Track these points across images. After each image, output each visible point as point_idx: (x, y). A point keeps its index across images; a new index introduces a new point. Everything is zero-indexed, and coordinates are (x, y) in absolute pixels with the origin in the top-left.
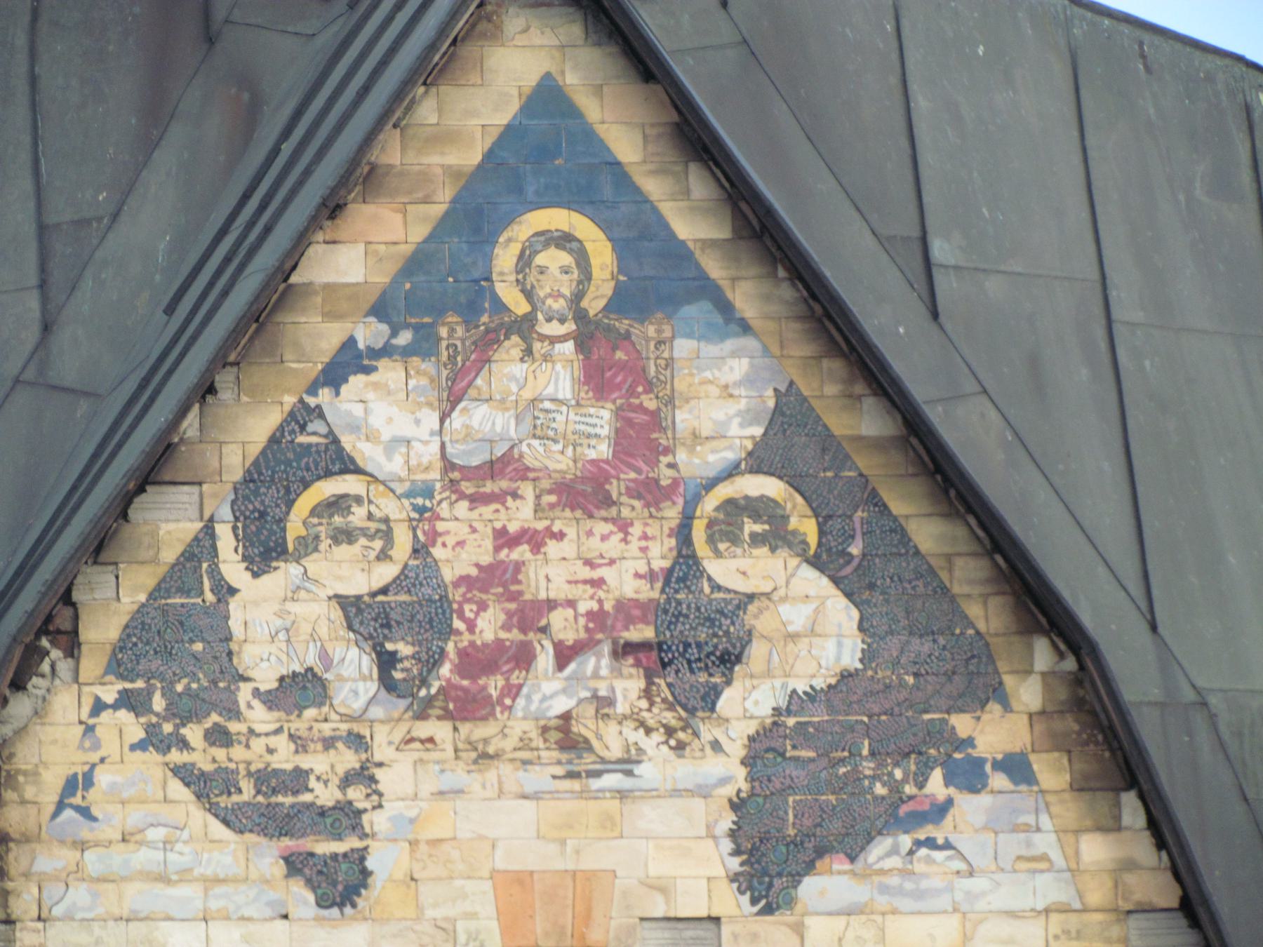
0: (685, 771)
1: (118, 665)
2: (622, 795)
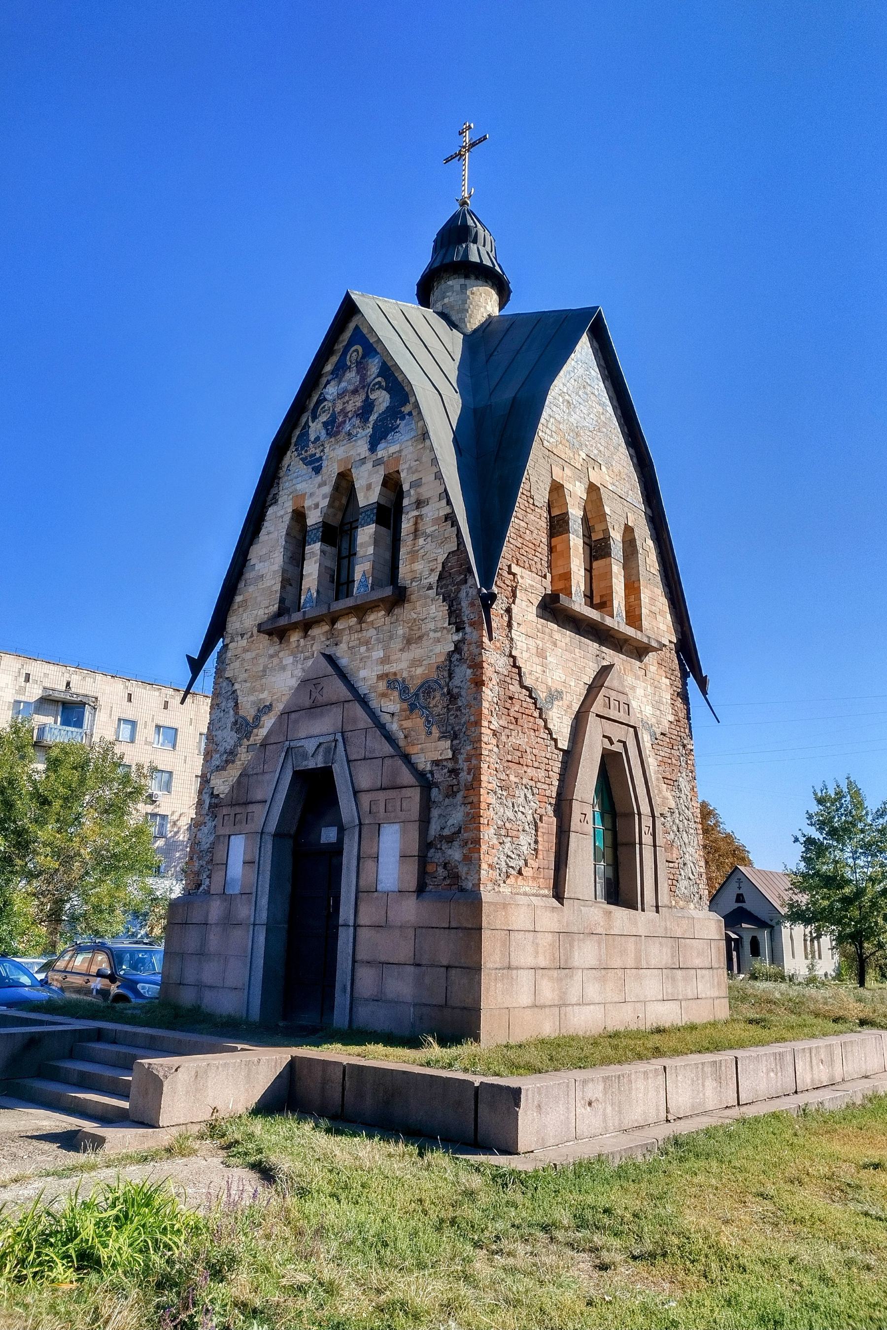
0: (364, 433)
1: (295, 445)
2: (355, 440)
